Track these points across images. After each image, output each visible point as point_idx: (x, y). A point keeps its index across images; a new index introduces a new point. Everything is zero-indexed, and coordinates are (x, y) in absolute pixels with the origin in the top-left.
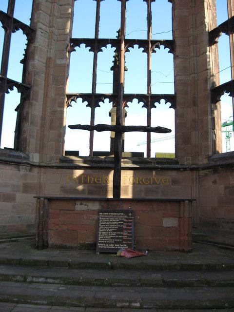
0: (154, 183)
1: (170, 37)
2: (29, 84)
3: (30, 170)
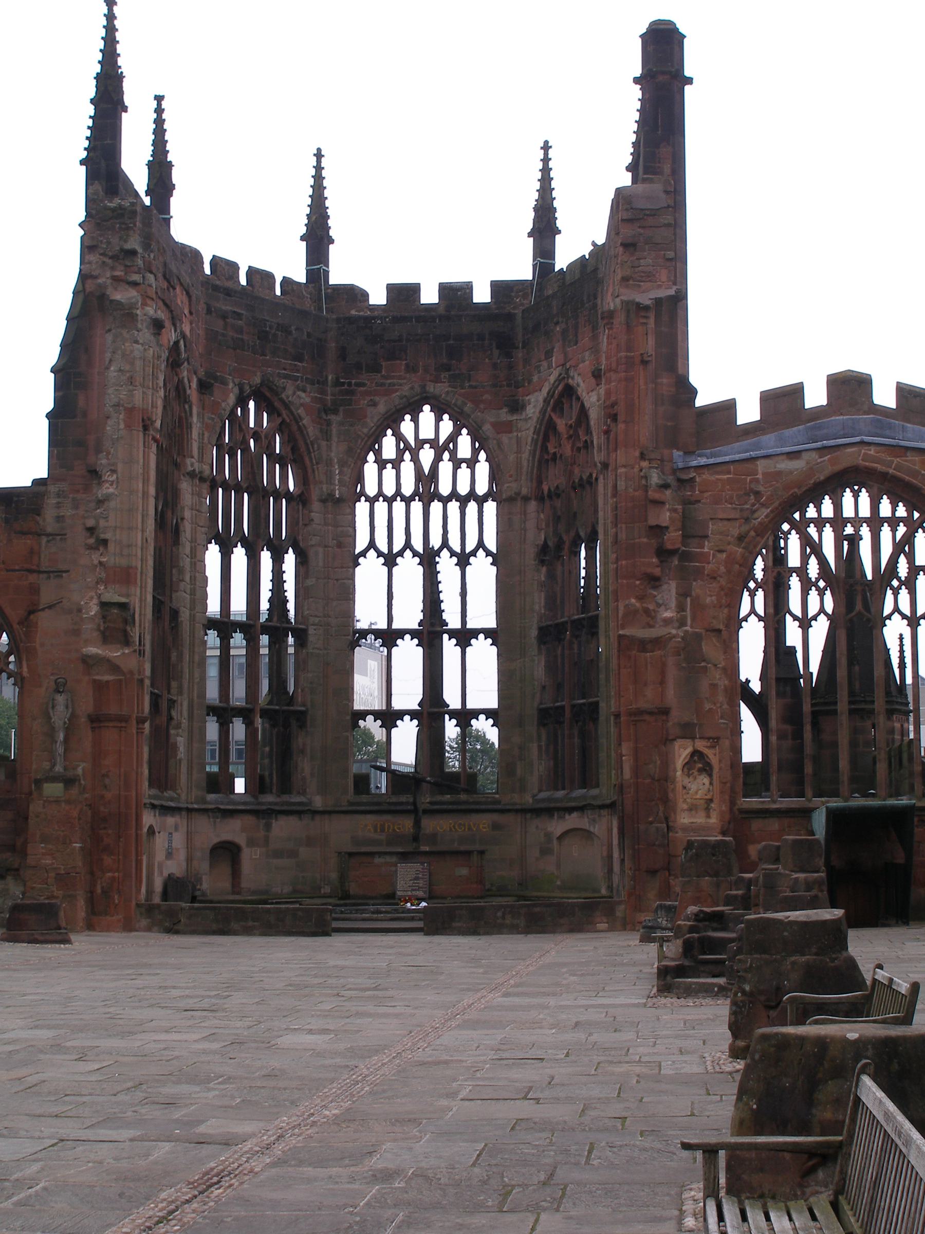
0: (470, 829)
1: (491, 623)
2: (304, 705)
3: (313, 819)
